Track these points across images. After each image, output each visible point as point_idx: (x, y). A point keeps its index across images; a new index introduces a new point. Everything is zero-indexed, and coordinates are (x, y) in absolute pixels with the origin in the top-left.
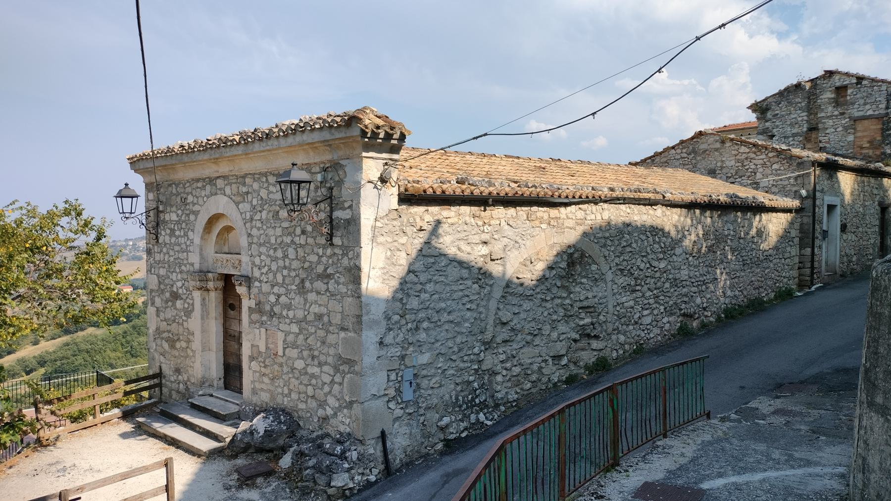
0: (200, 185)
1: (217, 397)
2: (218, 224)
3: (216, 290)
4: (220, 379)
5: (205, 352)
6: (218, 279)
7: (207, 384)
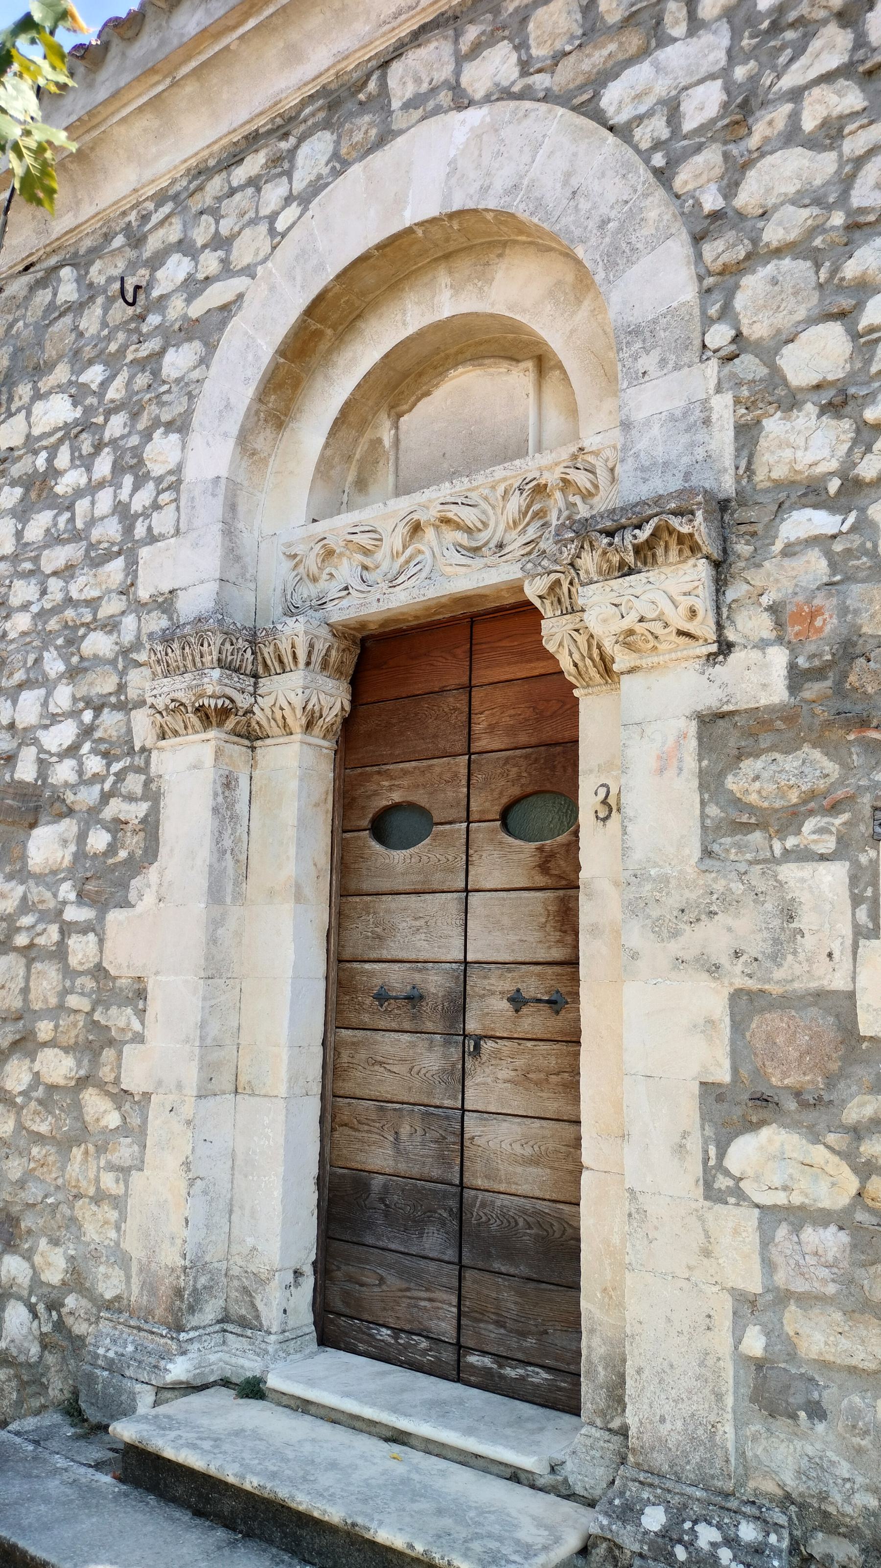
0: (254, 164)
1: (303, 1406)
2: (342, 359)
3: (309, 726)
4: (297, 1273)
5: (211, 1102)
6: (325, 665)
7: (210, 1312)
